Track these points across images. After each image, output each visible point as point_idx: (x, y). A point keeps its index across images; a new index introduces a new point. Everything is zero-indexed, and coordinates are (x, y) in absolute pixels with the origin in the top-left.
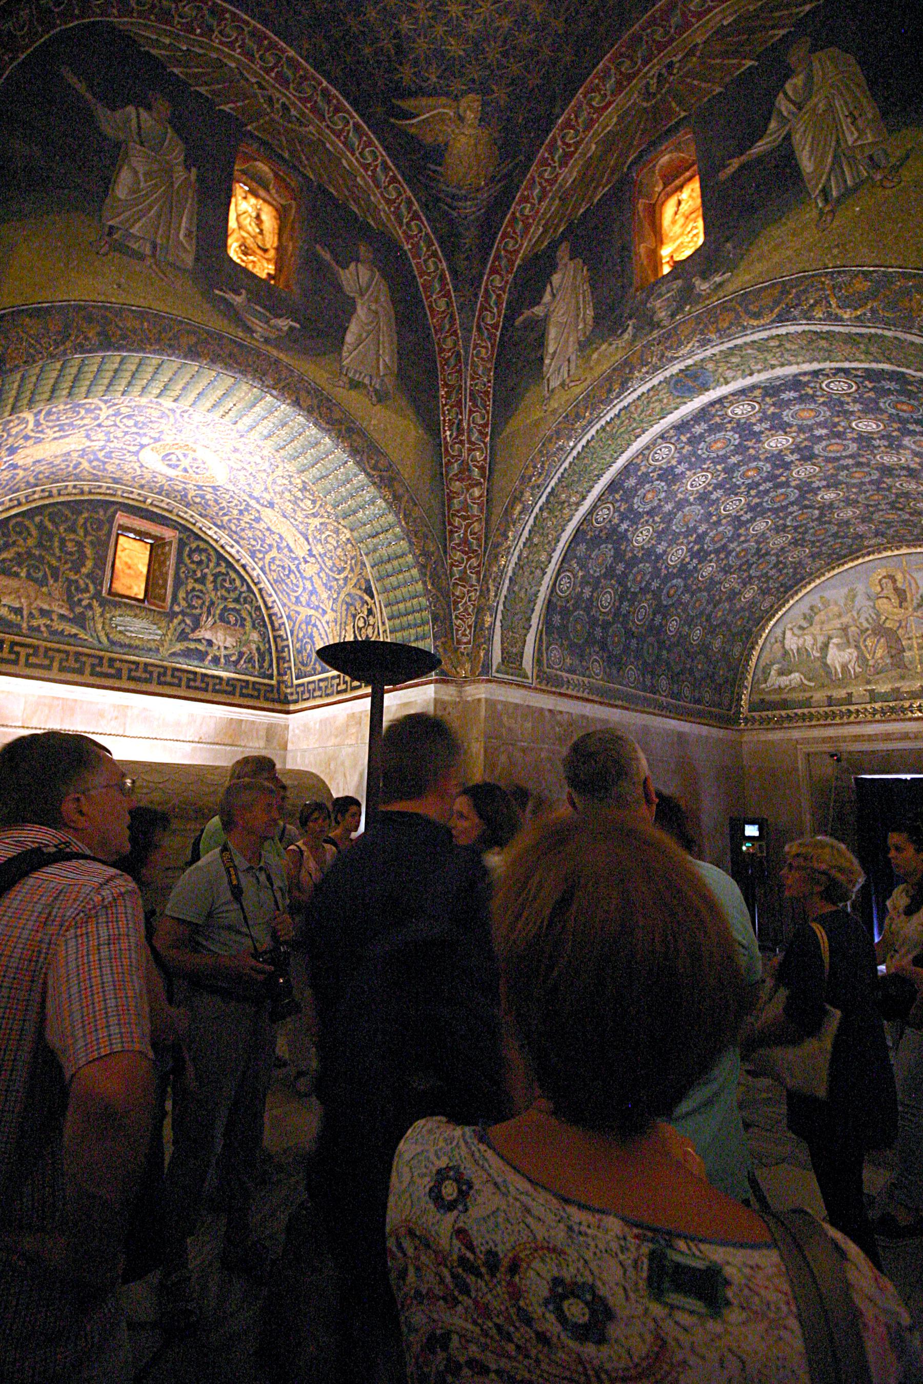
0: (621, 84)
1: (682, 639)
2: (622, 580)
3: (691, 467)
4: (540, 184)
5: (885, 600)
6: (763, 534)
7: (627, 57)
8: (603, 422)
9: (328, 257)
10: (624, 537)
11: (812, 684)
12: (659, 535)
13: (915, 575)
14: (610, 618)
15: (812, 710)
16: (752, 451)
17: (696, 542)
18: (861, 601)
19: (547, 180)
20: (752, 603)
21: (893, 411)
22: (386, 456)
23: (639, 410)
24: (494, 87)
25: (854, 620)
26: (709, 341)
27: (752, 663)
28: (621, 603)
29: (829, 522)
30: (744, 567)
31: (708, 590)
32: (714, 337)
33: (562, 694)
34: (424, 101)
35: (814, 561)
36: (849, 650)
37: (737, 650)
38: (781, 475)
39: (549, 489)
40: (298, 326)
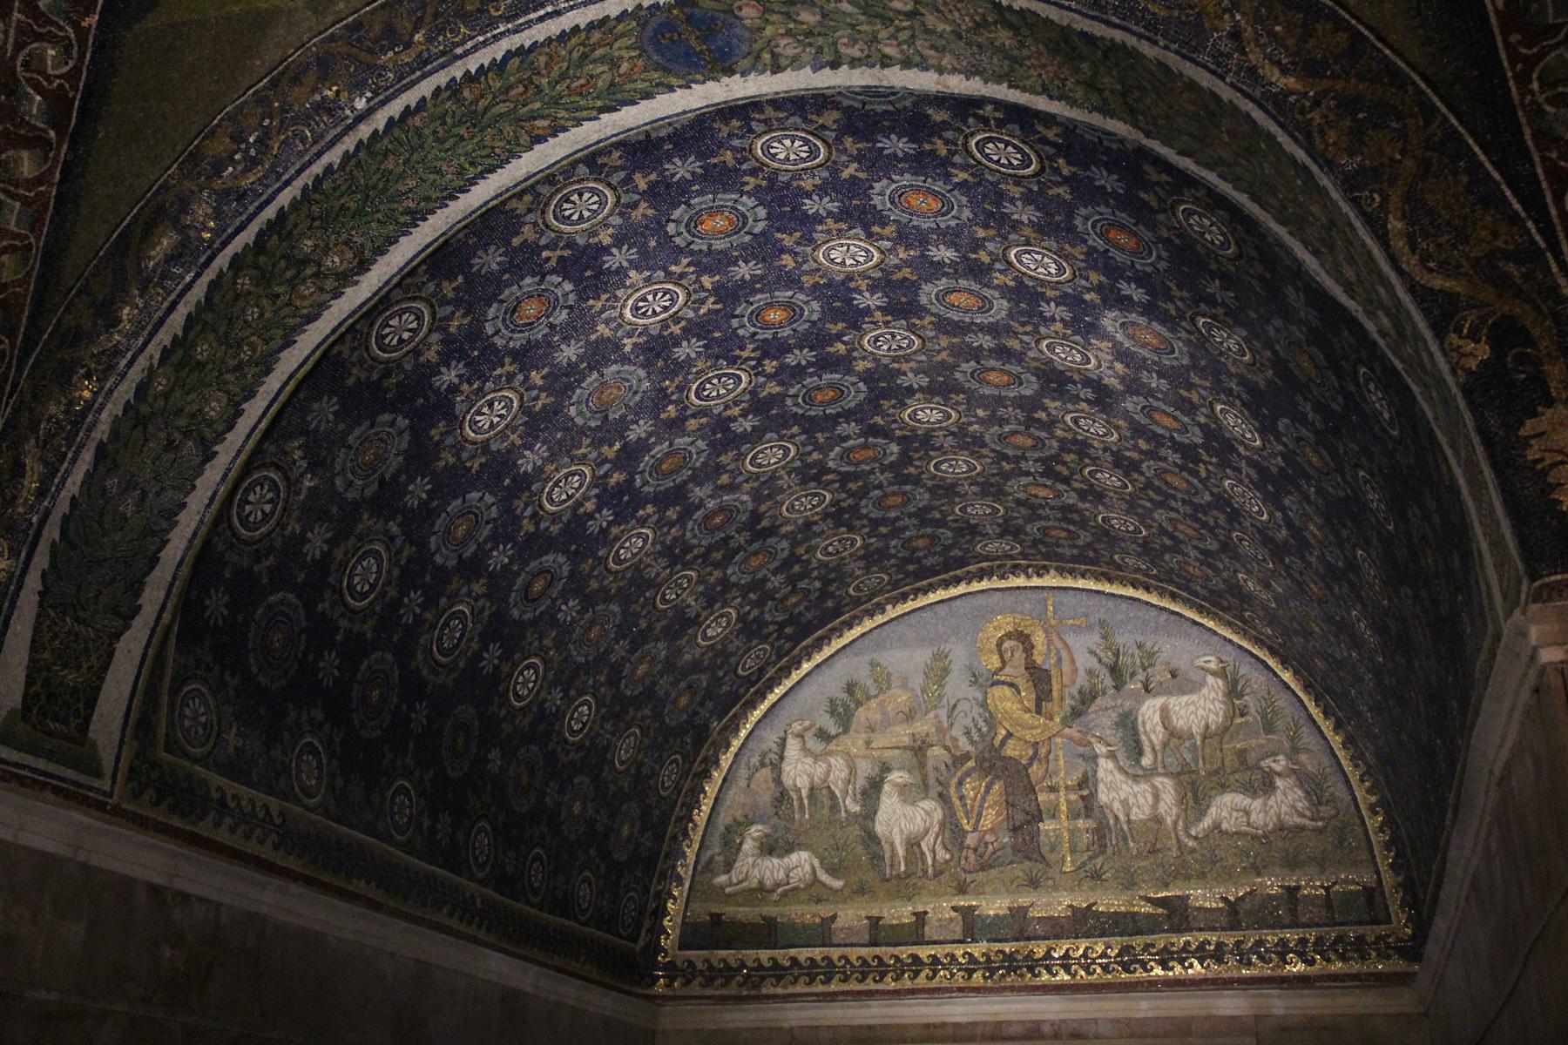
1: (545, 721)
2: (418, 522)
3: (644, 261)
5: (1007, 691)
6: (773, 477)
8: (457, 71)
10: (443, 407)
11: (837, 884)
12: (534, 424)
13: (1071, 640)
14: (368, 628)
15: (835, 953)
16: (787, 261)
17: (618, 464)
18: (957, 686)
20: (722, 655)
21: (1099, 244)
23: (555, 74)
25: (941, 731)
27: (701, 816)
28: (403, 593)
29: (916, 481)
30: (717, 556)
31: (625, 599)
33: (195, 840)
35: (867, 570)
36: (928, 805)
37: (668, 776)
38: (839, 337)
39: (270, 212)
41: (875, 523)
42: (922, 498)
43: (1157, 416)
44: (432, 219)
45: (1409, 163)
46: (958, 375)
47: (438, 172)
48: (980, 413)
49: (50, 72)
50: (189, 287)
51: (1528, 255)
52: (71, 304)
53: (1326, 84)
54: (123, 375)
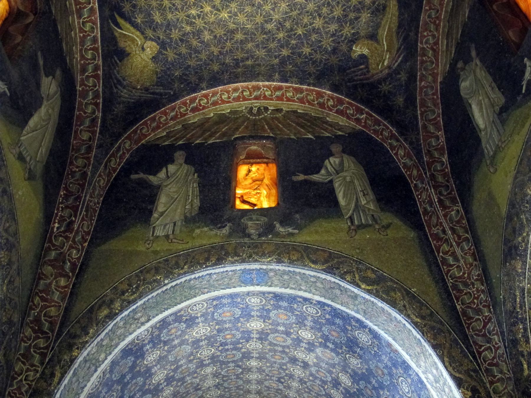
0: (239, 99)
3: (206, 321)
4: (177, 112)
6: (207, 375)
7: (250, 91)
9: (41, 62)
19: (180, 113)
22: (17, 224)
24: (168, 49)
26: (283, 262)
29: (241, 379)
32: (286, 260)
34: (128, 26)
40: (9, 94)
41: (225, 388)
42: (241, 382)
43: (320, 373)
44: (169, 310)
45: (447, 344)
46: (267, 356)
47: (176, 299)
48: (268, 364)
49: (73, 257)
50: (109, 325)
51: (475, 371)
52: (73, 325)
53: (426, 322)
54: (86, 349)
